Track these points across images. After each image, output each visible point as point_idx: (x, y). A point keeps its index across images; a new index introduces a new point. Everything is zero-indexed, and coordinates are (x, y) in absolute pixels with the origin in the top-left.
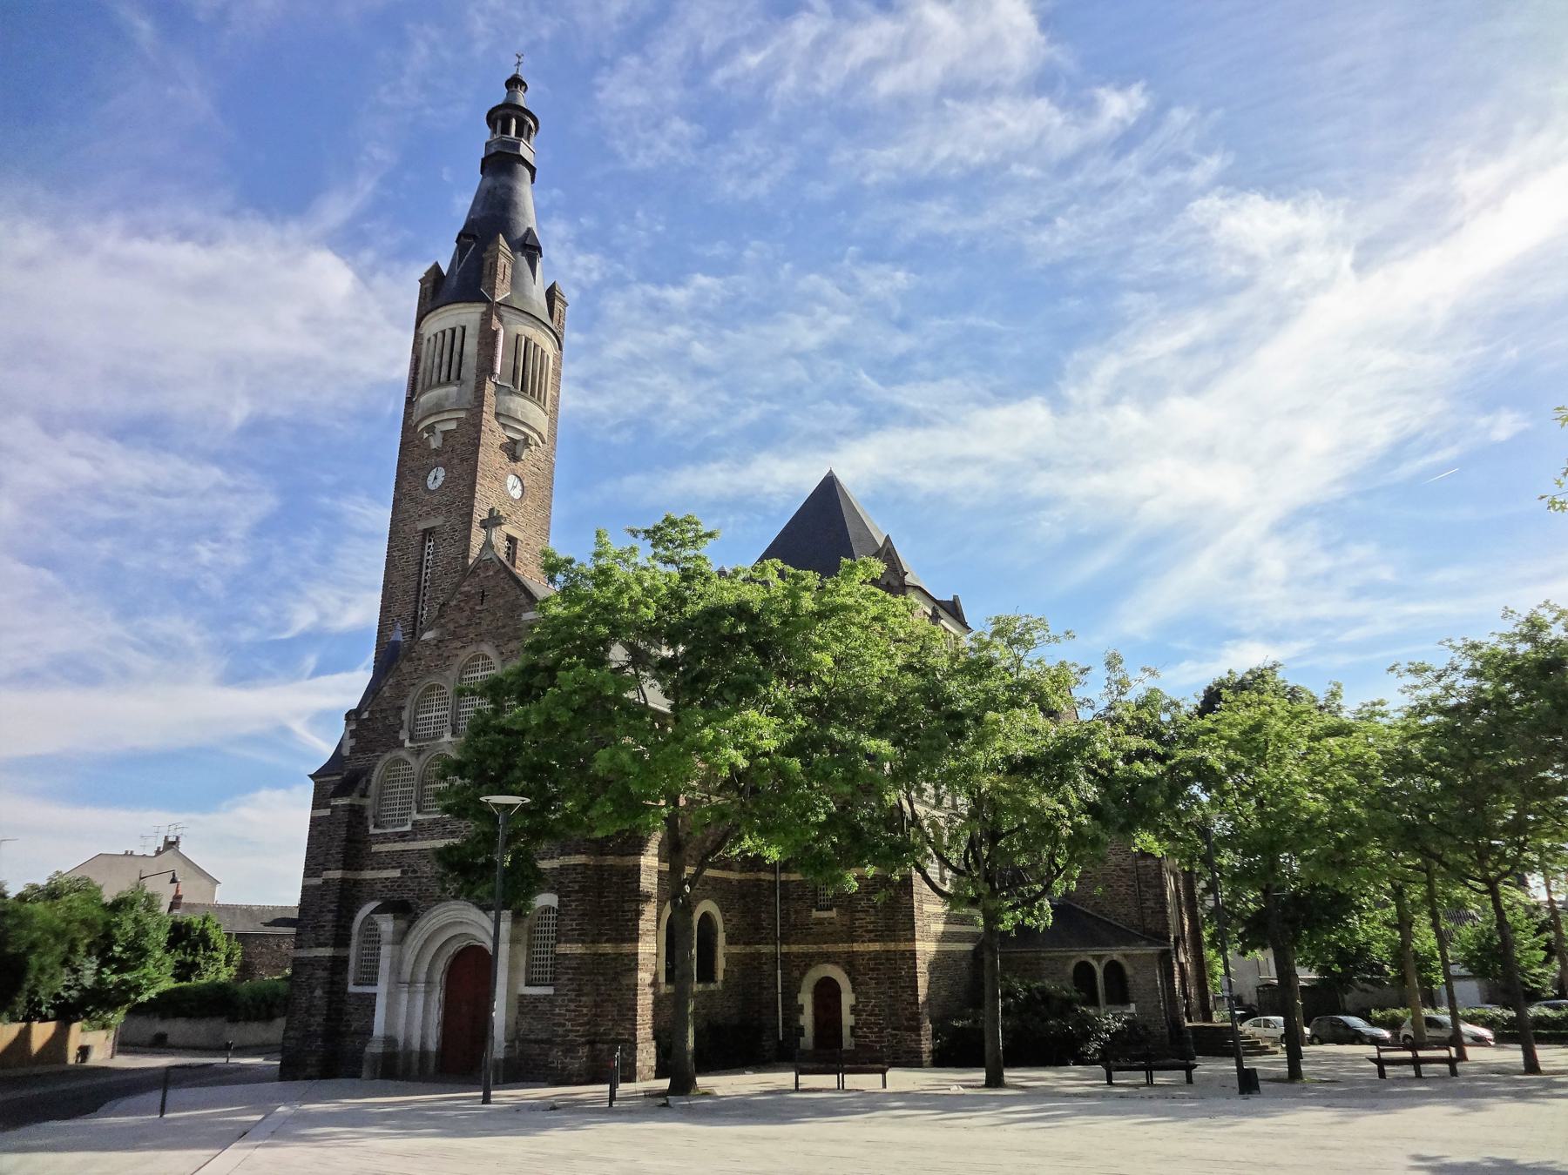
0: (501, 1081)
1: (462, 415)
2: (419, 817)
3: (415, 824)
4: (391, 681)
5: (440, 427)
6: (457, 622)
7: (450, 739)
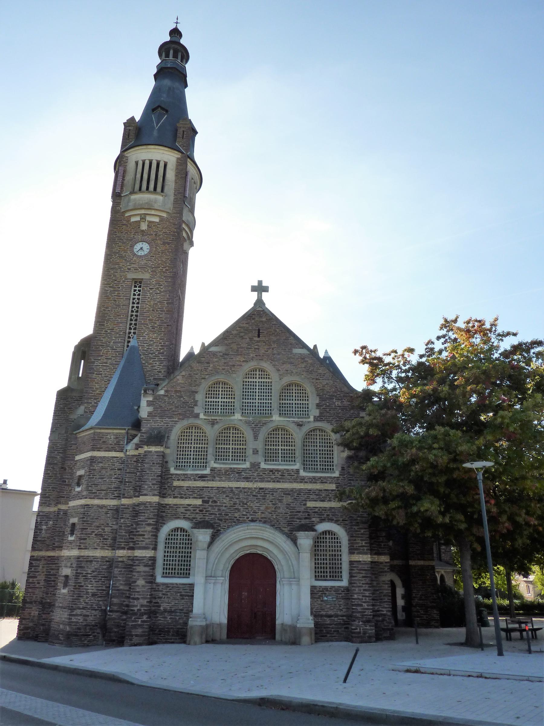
0: (313, 642)
1: (164, 215)
2: (216, 465)
3: (213, 470)
4: (183, 373)
5: (149, 218)
6: (239, 345)
7: (240, 418)
